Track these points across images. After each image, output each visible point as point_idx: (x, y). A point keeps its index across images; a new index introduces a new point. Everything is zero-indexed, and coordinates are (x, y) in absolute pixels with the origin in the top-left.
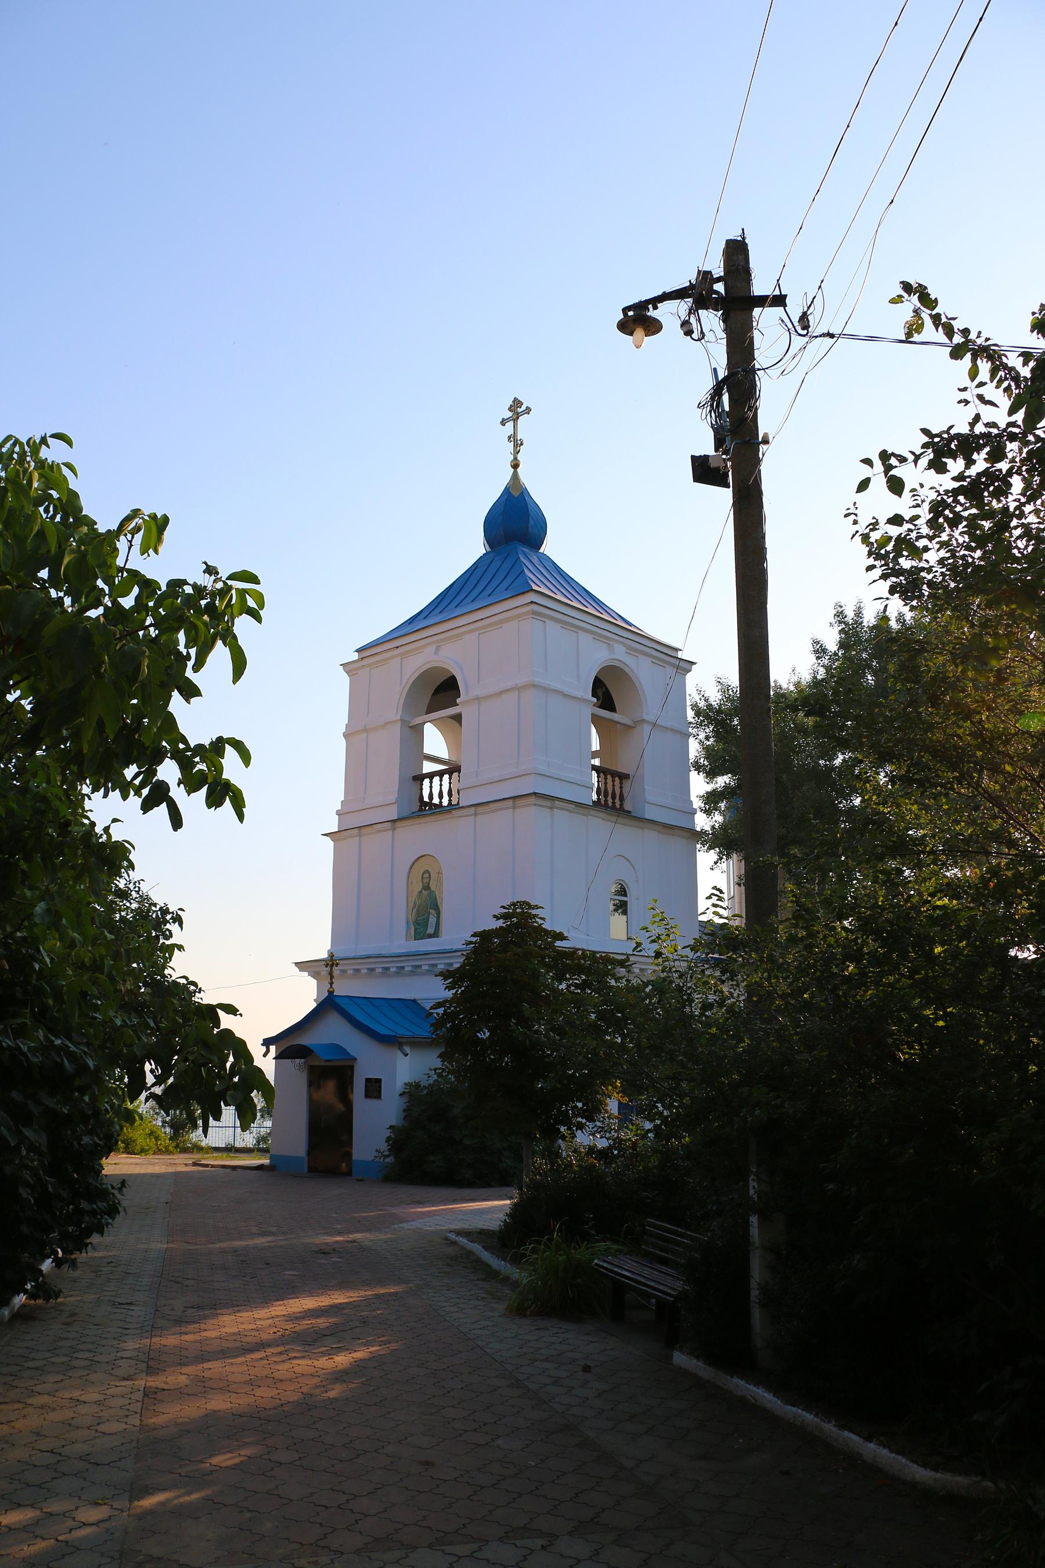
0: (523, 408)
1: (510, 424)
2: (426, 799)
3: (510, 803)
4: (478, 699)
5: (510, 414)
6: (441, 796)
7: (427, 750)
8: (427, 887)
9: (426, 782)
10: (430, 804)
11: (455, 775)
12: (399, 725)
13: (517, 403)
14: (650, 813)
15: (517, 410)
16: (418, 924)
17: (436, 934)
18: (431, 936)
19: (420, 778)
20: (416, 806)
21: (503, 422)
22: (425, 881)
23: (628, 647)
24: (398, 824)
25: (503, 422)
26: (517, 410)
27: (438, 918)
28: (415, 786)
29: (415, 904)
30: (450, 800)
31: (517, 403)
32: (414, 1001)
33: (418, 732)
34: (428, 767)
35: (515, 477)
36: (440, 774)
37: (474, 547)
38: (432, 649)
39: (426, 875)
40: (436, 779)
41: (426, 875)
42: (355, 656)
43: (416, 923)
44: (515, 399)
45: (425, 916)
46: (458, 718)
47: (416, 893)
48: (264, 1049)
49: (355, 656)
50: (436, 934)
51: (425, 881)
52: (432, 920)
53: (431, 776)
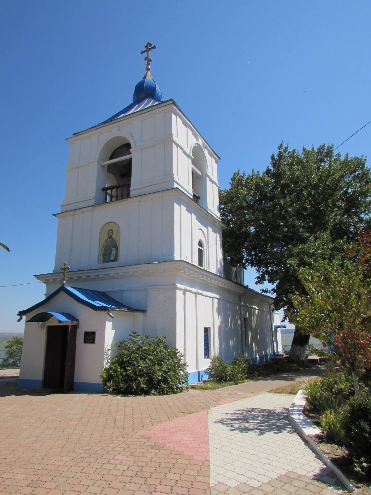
5: (145, 49)
8: (110, 237)
12: (97, 163)
15: (149, 47)
16: (105, 255)
17: (115, 260)
18: (113, 261)
22: (109, 234)
24: (96, 208)
26: (149, 47)
27: (117, 250)
29: (104, 245)
32: (103, 292)
39: (111, 232)
41: (111, 232)
43: (104, 255)
44: (148, 43)
45: (110, 250)
47: (104, 240)
48: (19, 317)
51: (109, 234)
52: (114, 253)
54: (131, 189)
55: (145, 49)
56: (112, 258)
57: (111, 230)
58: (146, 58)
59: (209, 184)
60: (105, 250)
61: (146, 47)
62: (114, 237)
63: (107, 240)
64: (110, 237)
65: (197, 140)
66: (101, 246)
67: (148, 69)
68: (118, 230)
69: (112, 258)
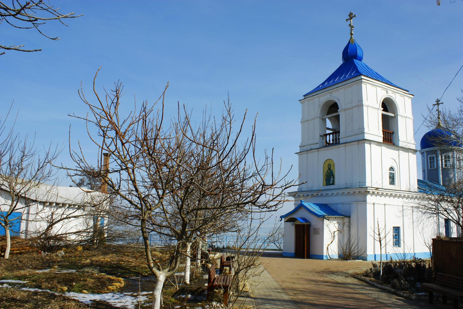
0: (354, 15)
1: (349, 21)
2: (328, 142)
3: (357, 142)
4: (345, 110)
5: (349, 18)
6: (333, 140)
7: (327, 126)
8: (329, 169)
9: (328, 136)
10: (329, 144)
11: (337, 134)
13: (351, 14)
14: (401, 144)
15: (351, 16)
17: (333, 184)
19: (326, 135)
20: (325, 144)
21: (347, 20)
23: (393, 91)
24: (319, 150)
25: (347, 20)
26: (351, 16)
28: (324, 137)
30: (336, 142)
31: (351, 14)
33: (324, 120)
34: (328, 132)
35: (351, 37)
36: (332, 134)
37: (339, 62)
38: (329, 95)
40: (331, 135)
42: (303, 98)
45: (329, 177)
46: (338, 117)
49: (303, 98)
50: (333, 184)
52: (332, 179)
53: (329, 134)
54: (340, 137)
55: (349, 18)
56: (331, 183)
57: (330, 164)
58: (350, 25)
59: (401, 121)
60: (327, 177)
61: (349, 15)
62: (332, 169)
63: (327, 171)
64: (329, 169)
65: (387, 92)
66: (325, 175)
67: (352, 34)
68: (334, 164)
69: (331, 183)
